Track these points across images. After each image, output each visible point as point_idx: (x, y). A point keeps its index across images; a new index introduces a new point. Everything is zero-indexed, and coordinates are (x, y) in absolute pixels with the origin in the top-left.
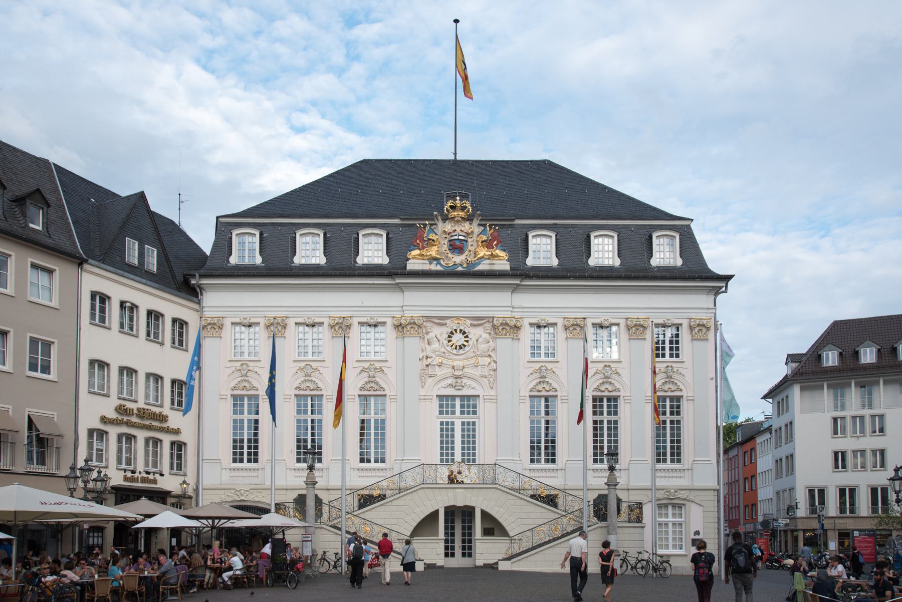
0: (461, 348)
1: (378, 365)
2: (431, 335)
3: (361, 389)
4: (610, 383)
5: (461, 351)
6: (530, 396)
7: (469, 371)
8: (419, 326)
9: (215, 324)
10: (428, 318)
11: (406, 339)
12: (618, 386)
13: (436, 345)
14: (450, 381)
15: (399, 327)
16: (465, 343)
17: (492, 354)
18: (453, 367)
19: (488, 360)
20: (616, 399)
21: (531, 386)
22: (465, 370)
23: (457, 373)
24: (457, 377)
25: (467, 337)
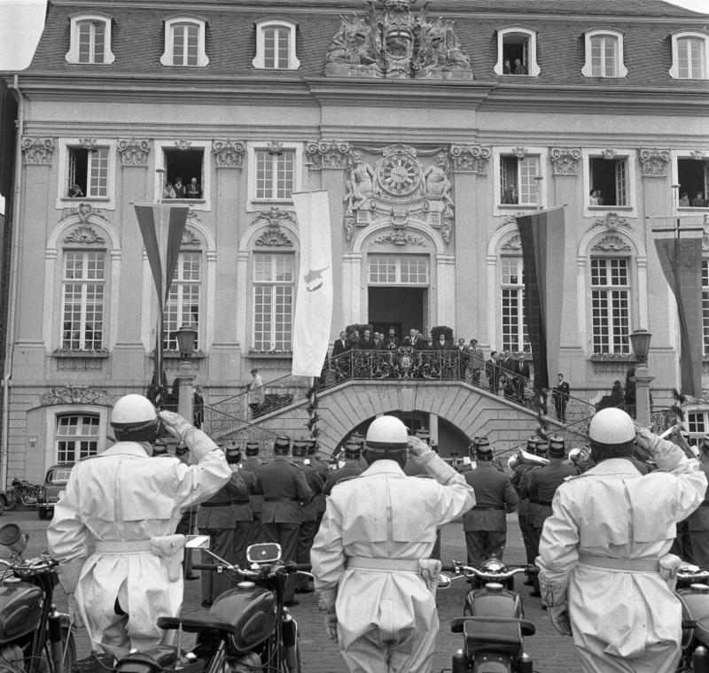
0: (403, 187)
1: (282, 209)
2: (358, 170)
3: (259, 242)
4: (617, 238)
5: (404, 192)
6: (502, 256)
7: (414, 222)
8: (343, 155)
9: (41, 146)
10: (357, 145)
11: (324, 174)
12: (629, 243)
13: (367, 184)
14: (387, 234)
15: (314, 156)
16: (411, 181)
17: (447, 196)
18: (392, 215)
19: (440, 206)
20: (624, 261)
21: (504, 242)
22: (410, 219)
23: (397, 223)
24: (397, 228)
25: (412, 171)
